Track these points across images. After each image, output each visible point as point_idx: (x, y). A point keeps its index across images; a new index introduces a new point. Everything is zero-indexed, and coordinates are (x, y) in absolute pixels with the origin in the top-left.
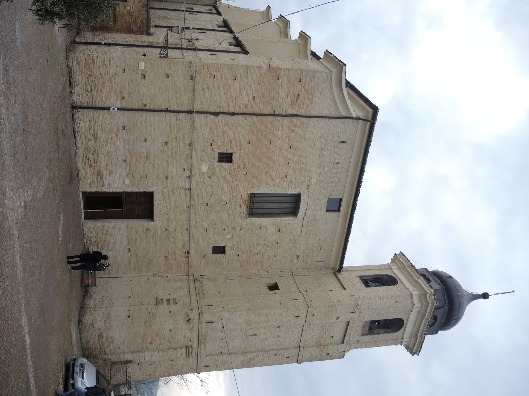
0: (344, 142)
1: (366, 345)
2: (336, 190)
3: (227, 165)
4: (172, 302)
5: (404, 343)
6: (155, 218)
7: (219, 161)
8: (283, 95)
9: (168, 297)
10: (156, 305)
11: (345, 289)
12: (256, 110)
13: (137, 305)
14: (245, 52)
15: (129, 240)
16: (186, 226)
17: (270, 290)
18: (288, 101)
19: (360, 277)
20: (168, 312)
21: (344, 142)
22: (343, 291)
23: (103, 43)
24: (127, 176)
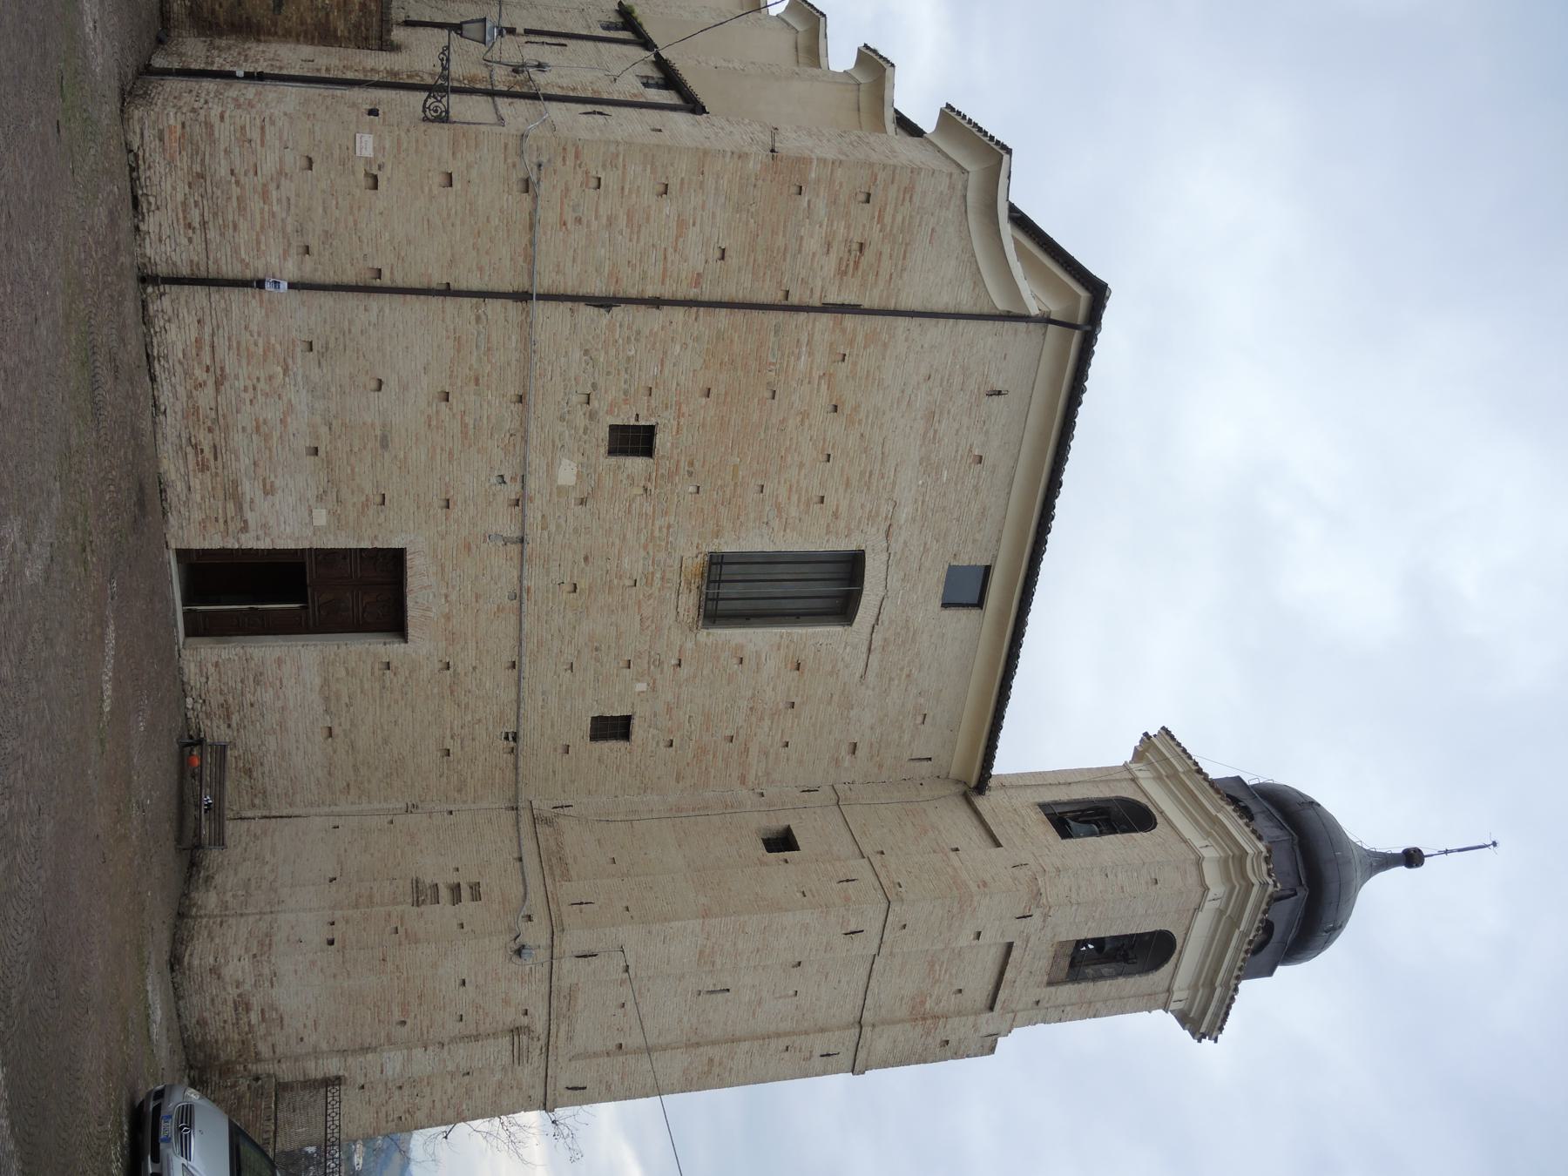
0: (999, 393)
1: (1062, 1014)
2: (974, 541)
3: (636, 464)
5: (1173, 1006)
6: (411, 631)
7: (612, 452)
8: (813, 244)
9: (453, 878)
10: (417, 903)
11: (998, 844)
12: (730, 291)
13: (357, 906)
14: (693, 105)
15: (327, 699)
16: (507, 656)
17: (769, 851)
18: (830, 264)
19: (1043, 807)
20: (455, 927)
21: (999, 393)
22: (994, 851)
23: (240, 73)
24: (320, 498)
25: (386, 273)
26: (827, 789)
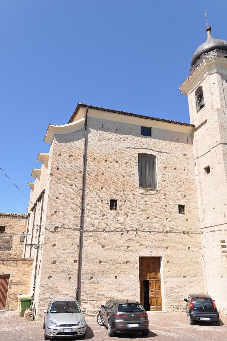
0: (102, 126)
2: (136, 130)
3: (118, 203)
7: (116, 209)
9: (220, 247)
12: (80, 183)
15: (177, 276)
16: (165, 234)
17: (210, 172)
21: (102, 126)
23: (33, 292)
24: (127, 276)
25: (75, 259)
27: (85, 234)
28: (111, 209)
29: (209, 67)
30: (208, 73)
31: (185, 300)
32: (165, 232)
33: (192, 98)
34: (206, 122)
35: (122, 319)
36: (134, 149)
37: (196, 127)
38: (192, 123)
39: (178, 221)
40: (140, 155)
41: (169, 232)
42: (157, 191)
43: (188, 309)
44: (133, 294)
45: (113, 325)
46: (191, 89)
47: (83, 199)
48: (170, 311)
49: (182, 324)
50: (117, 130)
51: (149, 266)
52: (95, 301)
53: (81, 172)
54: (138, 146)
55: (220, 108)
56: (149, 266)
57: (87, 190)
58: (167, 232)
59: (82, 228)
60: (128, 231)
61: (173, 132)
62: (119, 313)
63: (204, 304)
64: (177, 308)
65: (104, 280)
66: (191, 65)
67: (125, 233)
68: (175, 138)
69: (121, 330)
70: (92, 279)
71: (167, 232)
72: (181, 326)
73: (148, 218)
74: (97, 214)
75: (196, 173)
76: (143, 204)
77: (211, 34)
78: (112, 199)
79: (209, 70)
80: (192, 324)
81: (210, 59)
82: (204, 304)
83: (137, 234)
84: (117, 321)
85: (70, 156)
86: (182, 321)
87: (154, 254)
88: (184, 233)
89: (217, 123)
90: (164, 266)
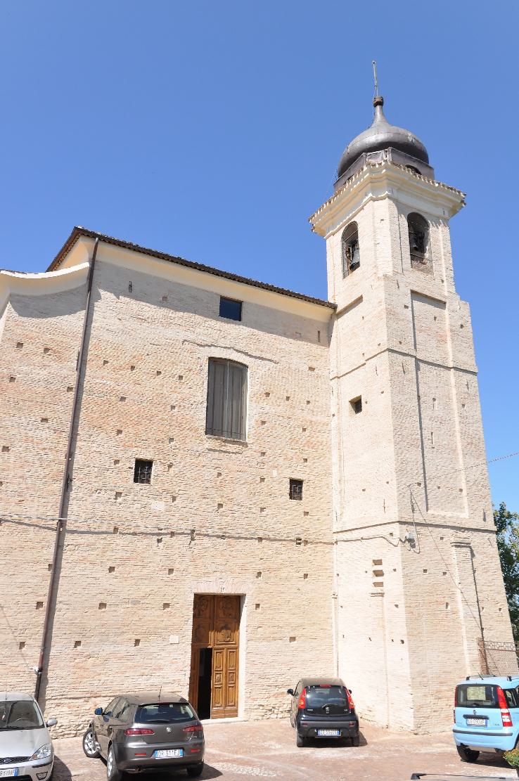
0: (131, 286)
4: (378, 568)
9: (371, 574)
10: (382, 595)
13: (383, 627)
15: (275, 639)
21: (131, 286)
25: (40, 599)
26: (331, 383)
27: (69, 539)
28: (136, 481)
29: (374, 184)
30: (370, 195)
31: (290, 692)
32: (256, 539)
33: (335, 246)
34: (360, 300)
35: (144, 741)
36: (201, 346)
37: (339, 310)
38: (331, 301)
39: (286, 515)
40: (213, 361)
41: (265, 539)
42: (245, 445)
43: (295, 712)
44: (174, 681)
45: (121, 754)
46: (333, 225)
47: (70, 454)
48: (256, 717)
49: (278, 746)
50: (165, 298)
51: (217, 614)
52: (82, 700)
53: (70, 389)
54: (209, 341)
55: (390, 274)
56: (217, 614)
57: (82, 432)
58: (260, 539)
59: (62, 524)
60: (173, 534)
61: (289, 315)
62: (136, 726)
63: (329, 700)
64: (270, 710)
65: (108, 649)
66: (336, 173)
67: (166, 539)
68: (293, 329)
69: (139, 766)
70: (79, 648)
71: (260, 539)
72: (275, 750)
73: (220, 505)
74: (103, 492)
75: (333, 410)
76: (210, 474)
77: (383, 114)
78: (141, 457)
79: (373, 190)
80: (300, 745)
81: (377, 166)
82: (329, 700)
83: (193, 542)
84: (132, 745)
85: (46, 350)
86: (279, 740)
87: (229, 589)
88: (298, 541)
89: (384, 306)
90: (248, 616)
